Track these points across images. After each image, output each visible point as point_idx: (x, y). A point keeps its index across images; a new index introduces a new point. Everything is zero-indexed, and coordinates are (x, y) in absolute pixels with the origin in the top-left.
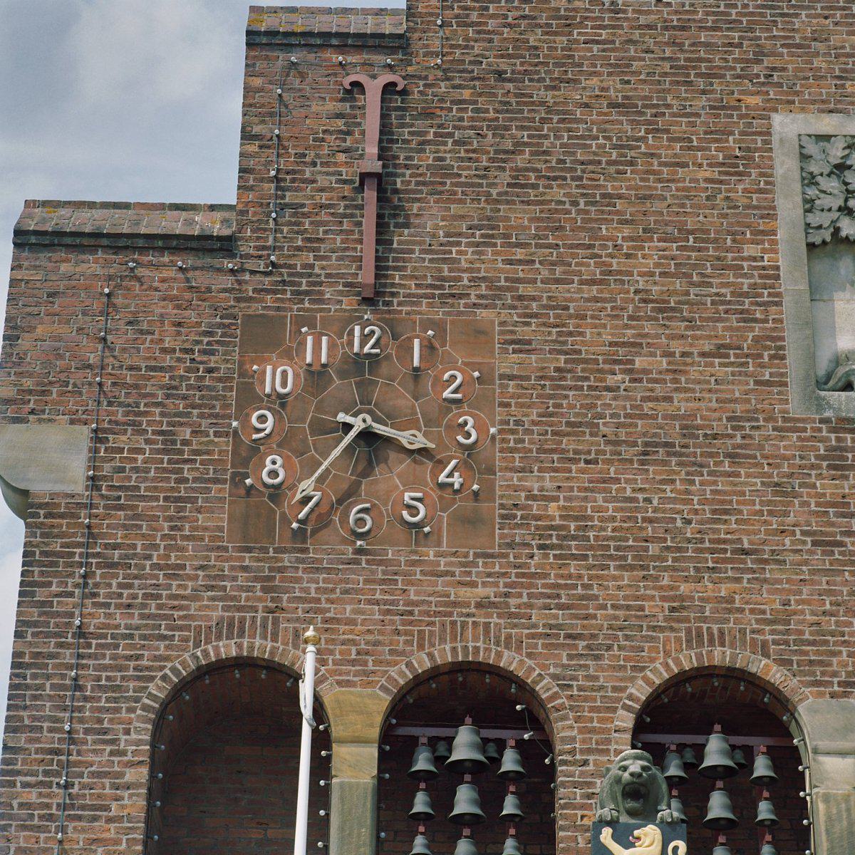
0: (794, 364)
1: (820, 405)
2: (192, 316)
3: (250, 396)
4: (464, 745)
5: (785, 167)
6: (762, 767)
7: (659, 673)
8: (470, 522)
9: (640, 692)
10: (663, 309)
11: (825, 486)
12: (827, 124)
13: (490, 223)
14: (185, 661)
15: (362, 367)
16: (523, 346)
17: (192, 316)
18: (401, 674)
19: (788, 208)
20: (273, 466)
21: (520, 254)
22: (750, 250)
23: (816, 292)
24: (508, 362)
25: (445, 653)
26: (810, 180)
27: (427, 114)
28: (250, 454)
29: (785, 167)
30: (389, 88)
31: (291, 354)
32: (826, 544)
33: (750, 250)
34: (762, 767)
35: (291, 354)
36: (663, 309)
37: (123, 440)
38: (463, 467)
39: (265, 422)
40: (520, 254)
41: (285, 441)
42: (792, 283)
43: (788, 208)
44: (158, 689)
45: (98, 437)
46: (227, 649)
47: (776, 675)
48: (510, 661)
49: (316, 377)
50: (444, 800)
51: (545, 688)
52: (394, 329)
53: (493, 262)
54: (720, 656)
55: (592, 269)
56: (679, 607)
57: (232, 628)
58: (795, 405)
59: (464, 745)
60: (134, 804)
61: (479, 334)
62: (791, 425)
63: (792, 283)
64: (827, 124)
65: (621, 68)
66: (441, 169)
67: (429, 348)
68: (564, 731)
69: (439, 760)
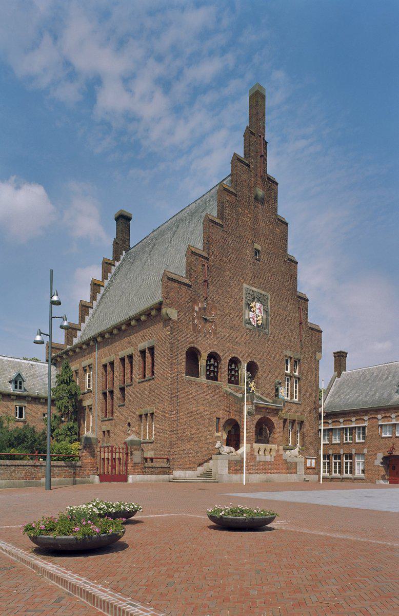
3: (194, 311)
5: (244, 292)
8: (215, 334)
11: (245, 336)
12: (248, 287)
13: (217, 291)
15: (205, 309)
19: (244, 298)
21: (220, 297)
22: (241, 303)
24: (218, 312)
27: (211, 272)
28: (194, 319)
29: (244, 292)
31: (198, 305)
33: (241, 303)
35: (198, 305)
37: (181, 313)
40: (220, 297)
43: (244, 298)
44: (186, 349)
45: (178, 313)
47: (240, 359)
48: (218, 352)
54: (236, 356)
56: (233, 348)
57: (193, 343)
58: (243, 325)
60: (184, 364)
61: (215, 307)
65: (230, 271)
67: (211, 308)
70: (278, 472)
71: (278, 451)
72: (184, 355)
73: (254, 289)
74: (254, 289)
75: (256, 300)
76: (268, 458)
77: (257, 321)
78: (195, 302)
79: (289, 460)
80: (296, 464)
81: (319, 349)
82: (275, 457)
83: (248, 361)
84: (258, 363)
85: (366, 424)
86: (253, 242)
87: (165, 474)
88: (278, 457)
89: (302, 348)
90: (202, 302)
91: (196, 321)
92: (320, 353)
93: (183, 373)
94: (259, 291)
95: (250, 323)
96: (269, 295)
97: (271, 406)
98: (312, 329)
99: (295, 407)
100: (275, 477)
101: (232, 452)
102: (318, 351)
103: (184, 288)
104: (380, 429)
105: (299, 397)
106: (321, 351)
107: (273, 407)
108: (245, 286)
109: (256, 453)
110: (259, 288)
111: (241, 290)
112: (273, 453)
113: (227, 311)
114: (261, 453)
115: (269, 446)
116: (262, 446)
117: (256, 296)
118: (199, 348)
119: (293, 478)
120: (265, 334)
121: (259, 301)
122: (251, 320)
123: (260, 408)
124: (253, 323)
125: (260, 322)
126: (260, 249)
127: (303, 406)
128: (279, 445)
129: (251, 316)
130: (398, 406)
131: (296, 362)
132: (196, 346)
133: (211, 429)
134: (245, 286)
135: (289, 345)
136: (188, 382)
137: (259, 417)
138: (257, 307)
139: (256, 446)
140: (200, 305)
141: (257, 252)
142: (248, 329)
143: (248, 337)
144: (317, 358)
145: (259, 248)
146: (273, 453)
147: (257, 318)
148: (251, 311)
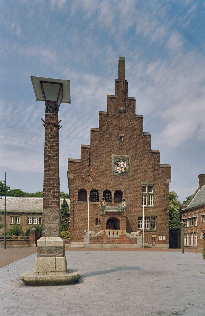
0: (112, 172)
1: (114, 174)
2: (79, 167)
3: (82, 173)
4: (94, 194)
5: (113, 158)
6: (109, 195)
7: (104, 190)
8: (95, 181)
9: (103, 191)
10: (106, 168)
12: (115, 155)
14: (79, 189)
15: (88, 171)
16: (97, 170)
17: (79, 167)
18: (91, 190)
19: (113, 161)
20: (84, 177)
23: (114, 167)
24: (97, 171)
25: (93, 189)
26: (114, 159)
28: (82, 176)
29: (113, 158)
30: (90, 152)
31: (84, 170)
32: (114, 183)
34: (109, 195)
35: (84, 170)
36: (106, 168)
37: (75, 175)
38: (94, 177)
39: (83, 174)
41: (84, 176)
42: (113, 166)
43: (113, 161)
45: (74, 175)
46: (82, 188)
47: (110, 190)
48: (97, 189)
49: (86, 171)
50: (93, 196)
51: (98, 191)
52: (90, 169)
53: (96, 164)
54: (108, 189)
55: (101, 165)
56: (106, 186)
59: (94, 194)
60: (77, 196)
61: (95, 169)
62: (112, 175)
63: (113, 166)
64: (115, 155)
66: (93, 157)
67: (92, 170)
68: (99, 193)
69: (93, 194)
70: (122, 242)
71: (122, 233)
72: (77, 193)
73: (119, 155)
74: (119, 155)
75: (121, 161)
76: (115, 236)
77: (122, 170)
78: (83, 169)
79: (130, 237)
80: (136, 239)
81: (169, 177)
82: (120, 236)
83: (116, 190)
84: (122, 191)
85: (197, 216)
86: (118, 134)
87: (67, 244)
88: (122, 235)
89: (154, 178)
90: (87, 168)
91: (84, 177)
92: (169, 180)
93: (77, 201)
94: (123, 156)
95: (117, 172)
96: (130, 156)
97: (115, 212)
98: (163, 167)
99: (150, 210)
100: (121, 245)
101: (92, 234)
102: (168, 179)
103: (77, 164)
104: (202, 218)
105: (154, 204)
106: (170, 178)
107: (117, 212)
108: (113, 155)
109: (107, 234)
110: (123, 154)
111: (110, 158)
112: (119, 234)
113: (102, 169)
114: (111, 234)
115: (116, 231)
116: (112, 231)
117: (121, 159)
118: (85, 189)
119: (134, 245)
120: (127, 176)
121: (123, 160)
122: (118, 171)
123: (108, 213)
124: (119, 172)
125: (124, 171)
126: (123, 136)
127: (155, 209)
128: (123, 230)
129: (117, 169)
130: (204, 205)
131: (150, 187)
132: (83, 188)
133: (93, 224)
134: (113, 155)
135: (144, 179)
136: (79, 204)
137: (109, 217)
138: (122, 164)
139: (107, 231)
140: (86, 170)
141: (121, 138)
142: (115, 175)
143: (116, 179)
144: (167, 182)
145: (123, 135)
146: (119, 234)
147: (122, 169)
148: (118, 167)
